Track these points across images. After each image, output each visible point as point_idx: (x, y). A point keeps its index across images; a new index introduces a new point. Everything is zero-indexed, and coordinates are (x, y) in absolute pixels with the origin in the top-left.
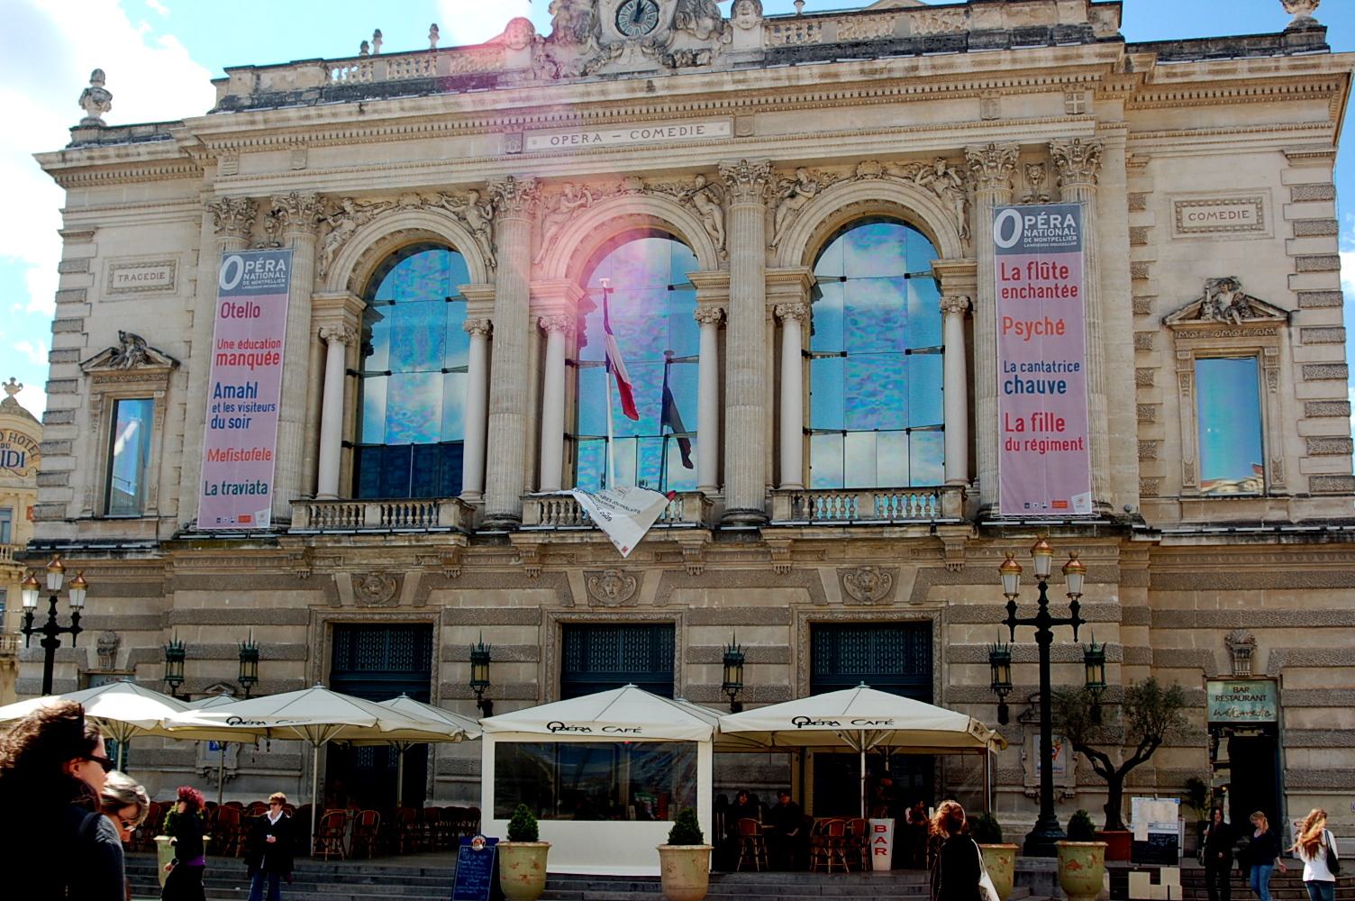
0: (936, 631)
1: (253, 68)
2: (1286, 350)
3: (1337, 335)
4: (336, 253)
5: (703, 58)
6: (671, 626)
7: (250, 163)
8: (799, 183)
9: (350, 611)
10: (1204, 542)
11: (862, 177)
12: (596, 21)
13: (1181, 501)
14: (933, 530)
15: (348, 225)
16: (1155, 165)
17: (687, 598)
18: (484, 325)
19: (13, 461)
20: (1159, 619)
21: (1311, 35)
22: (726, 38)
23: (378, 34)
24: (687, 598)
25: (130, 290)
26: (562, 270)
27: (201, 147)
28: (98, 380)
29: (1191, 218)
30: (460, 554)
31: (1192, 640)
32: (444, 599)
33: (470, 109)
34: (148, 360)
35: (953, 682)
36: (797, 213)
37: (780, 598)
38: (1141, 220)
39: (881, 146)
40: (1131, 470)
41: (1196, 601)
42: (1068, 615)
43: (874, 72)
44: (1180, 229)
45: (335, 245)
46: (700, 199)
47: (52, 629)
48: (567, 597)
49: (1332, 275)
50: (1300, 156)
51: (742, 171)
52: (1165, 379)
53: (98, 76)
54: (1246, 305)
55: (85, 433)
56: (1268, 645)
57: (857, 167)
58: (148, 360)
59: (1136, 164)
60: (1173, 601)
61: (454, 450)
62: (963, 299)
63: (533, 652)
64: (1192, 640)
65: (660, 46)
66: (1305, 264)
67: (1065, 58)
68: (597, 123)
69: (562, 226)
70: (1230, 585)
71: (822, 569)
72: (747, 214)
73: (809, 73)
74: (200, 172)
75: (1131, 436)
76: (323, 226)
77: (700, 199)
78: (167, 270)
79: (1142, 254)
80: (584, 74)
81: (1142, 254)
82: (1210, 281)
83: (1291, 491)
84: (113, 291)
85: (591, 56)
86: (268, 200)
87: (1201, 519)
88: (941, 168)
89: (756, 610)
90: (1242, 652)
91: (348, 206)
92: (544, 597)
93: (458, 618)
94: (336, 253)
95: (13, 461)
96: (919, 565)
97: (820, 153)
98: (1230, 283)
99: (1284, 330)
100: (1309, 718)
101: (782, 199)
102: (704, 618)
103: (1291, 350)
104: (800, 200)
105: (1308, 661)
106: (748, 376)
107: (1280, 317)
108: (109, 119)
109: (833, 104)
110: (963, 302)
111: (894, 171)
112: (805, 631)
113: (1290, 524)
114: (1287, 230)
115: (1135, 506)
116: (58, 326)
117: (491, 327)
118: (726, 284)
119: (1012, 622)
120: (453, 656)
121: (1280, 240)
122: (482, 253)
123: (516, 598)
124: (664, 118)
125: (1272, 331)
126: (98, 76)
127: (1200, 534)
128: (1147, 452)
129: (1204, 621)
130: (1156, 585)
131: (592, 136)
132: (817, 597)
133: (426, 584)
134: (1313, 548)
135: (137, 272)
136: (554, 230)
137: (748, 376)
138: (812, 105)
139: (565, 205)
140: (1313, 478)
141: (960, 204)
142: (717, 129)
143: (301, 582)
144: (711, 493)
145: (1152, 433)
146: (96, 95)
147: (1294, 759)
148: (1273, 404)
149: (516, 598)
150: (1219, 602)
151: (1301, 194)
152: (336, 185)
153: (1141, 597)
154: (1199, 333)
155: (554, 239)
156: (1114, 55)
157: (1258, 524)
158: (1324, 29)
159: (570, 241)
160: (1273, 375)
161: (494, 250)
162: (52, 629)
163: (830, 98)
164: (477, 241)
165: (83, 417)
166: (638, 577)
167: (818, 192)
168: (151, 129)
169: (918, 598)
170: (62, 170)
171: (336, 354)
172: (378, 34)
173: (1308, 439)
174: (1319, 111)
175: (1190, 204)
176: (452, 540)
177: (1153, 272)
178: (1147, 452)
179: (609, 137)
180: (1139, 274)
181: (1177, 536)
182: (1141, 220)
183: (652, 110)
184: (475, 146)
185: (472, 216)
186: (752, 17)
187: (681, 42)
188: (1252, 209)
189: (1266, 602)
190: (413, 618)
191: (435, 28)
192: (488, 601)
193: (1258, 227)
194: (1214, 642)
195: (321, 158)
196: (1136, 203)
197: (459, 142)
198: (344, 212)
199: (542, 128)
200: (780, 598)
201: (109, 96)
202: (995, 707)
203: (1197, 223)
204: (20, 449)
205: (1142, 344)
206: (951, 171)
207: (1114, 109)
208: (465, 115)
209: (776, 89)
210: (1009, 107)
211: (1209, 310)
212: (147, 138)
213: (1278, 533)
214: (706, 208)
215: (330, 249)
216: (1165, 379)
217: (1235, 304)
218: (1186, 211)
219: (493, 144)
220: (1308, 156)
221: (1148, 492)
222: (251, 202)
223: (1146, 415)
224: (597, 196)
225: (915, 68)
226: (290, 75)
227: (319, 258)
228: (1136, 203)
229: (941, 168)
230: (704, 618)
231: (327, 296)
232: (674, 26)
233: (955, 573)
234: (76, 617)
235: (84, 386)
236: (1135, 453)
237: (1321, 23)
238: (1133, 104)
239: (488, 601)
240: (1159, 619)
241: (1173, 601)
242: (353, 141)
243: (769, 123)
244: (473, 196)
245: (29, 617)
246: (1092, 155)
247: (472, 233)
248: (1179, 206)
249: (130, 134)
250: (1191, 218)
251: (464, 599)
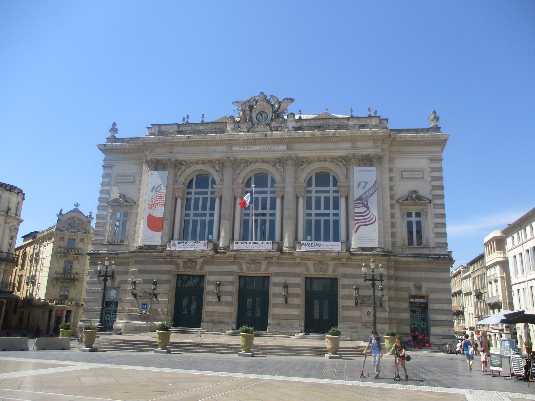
0: (338, 280)
1: (159, 125)
2: (429, 210)
3: (443, 206)
4: (180, 175)
5: (279, 129)
6: (269, 277)
7: (157, 150)
8: (303, 162)
9: (182, 271)
10: (408, 259)
11: (320, 161)
12: (251, 118)
13: (403, 247)
14: (339, 254)
15: (183, 168)
16: (396, 161)
17: (273, 270)
18: (220, 196)
19: (76, 225)
20: (397, 278)
21: (437, 129)
22: (286, 124)
23: (188, 116)
24: (273, 270)
25: (122, 182)
26: (241, 182)
27: (145, 145)
28: (112, 206)
29: (405, 175)
30: (213, 257)
31: (405, 284)
32: (208, 268)
33: (218, 139)
34: (127, 201)
35: (343, 294)
36: (303, 170)
37: (298, 270)
38: (392, 175)
39: (326, 154)
40: (389, 239)
41: (406, 274)
42: (380, 278)
43: (324, 134)
44: (402, 178)
45: (180, 173)
46: (277, 165)
47: (106, 276)
48: (241, 269)
49: (441, 191)
50: (434, 160)
51: (289, 158)
52: (398, 216)
53: (115, 124)
54: (419, 198)
55: (109, 220)
56: (425, 286)
58: (127, 201)
59: (391, 160)
60: (400, 274)
62: (346, 194)
63: (232, 283)
64: (405, 284)
65: (269, 125)
66: (434, 188)
67: (374, 133)
68: (251, 144)
69: (241, 170)
70: (415, 270)
71: (309, 262)
72: (290, 169)
73: (308, 133)
74: (143, 152)
75: (389, 231)
76: (177, 168)
77: (277, 165)
78: (132, 178)
79: (393, 184)
80: (248, 131)
81: (393, 184)
82: (410, 191)
83: (431, 246)
84: (117, 183)
85: (250, 126)
86: (162, 160)
87: (407, 253)
88: (340, 160)
89: (291, 273)
90: (419, 288)
91: (184, 163)
92: (235, 268)
93: (211, 273)
94: (180, 175)
95: (76, 225)
96: (334, 262)
97: (310, 155)
98: (415, 192)
99: (429, 205)
100: (436, 306)
101: (299, 166)
102: (277, 275)
103: (431, 210)
104: (304, 166)
105: (435, 290)
106: (289, 212)
107: (428, 201)
108: (117, 136)
109: (313, 142)
110: (346, 194)
111: (328, 160)
112: (304, 279)
113: (430, 255)
114: (429, 179)
115: (390, 249)
116: (101, 192)
117: (222, 196)
118: (284, 187)
119: (365, 280)
120: (211, 283)
121: (428, 181)
122: (220, 176)
123: (228, 268)
124: (269, 144)
125: (426, 205)
126: (115, 124)
127: (407, 257)
128: (393, 234)
129: (408, 279)
130: (396, 269)
131: (250, 147)
132: (308, 270)
133: (203, 264)
134: (436, 261)
135: (124, 178)
136: (239, 171)
137: (289, 212)
138: (308, 142)
139: (242, 165)
140: (437, 243)
141: (345, 169)
142: (283, 147)
143: (171, 263)
144: (280, 242)
145: (395, 230)
146: (114, 129)
147: (432, 316)
148: (426, 224)
149: (228, 268)
150: (412, 274)
151: (434, 170)
152: (181, 157)
153: (392, 272)
154: (407, 205)
155: (239, 174)
156: (387, 133)
157: (422, 254)
158: (440, 128)
159: (243, 175)
160: (426, 216)
161: (223, 176)
162: (106, 276)
163: (313, 140)
164: (218, 174)
166: (260, 263)
167: (308, 164)
168: (129, 139)
169: (334, 271)
170: (104, 149)
171: (179, 202)
172: (188, 116)
173: (436, 233)
174: (439, 149)
175: (404, 171)
176: (211, 252)
177: (395, 188)
178: (393, 234)
179: (254, 148)
180: (391, 188)
181: (401, 257)
182: (392, 175)
183: (266, 141)
184: (219, 148)
185: (217, 167)
186: (293, 119)
188: (421, 173)
189: (424, 275)
190: (199, 274)
191: (203, 115)
192: (219, 269)
193: (422, 178)
194: (411, 285)
195: (177, 149)
196: (391, 170)
197: (214, 148)
198: (182, 164)
199: (237, 145)
200: (298, 270)
201: (117, 130)
202: (354, 301)
203: (406, 176)
204: (78, 222)
205: (392, 206)
206: (343, 161)
207: (386, 146)
208: (216, 141)
209: (299, 138)
210: (359, 144)
211: (409, 199)
212: (128, 141)
213: (428, 257)
214: (279, 167)
215: (179, 174)
216: (398, 216)
217: (416, 197)
218: (404, 173)
219: (224, 148)
220: (435, 160)
221: (394, 245)
222: (158, 161)
223: (393, 225)
224: (250, 163)
225: (335, 134)
226: (169, 127)
227: (175, 176)
228: (391, 170)
229: (340, 160)
230: (277, 275)
231: (178, 186)
232: (272, 120)
233: (344, 265)
234: (113, 273)
236: (390, 234)
237: (439, 126)
238: (391, 145)
239: (219, 269)
240: (397, 278)
241: (400, 274)
242: (186, 146)
243: (296, 146)
244: (217, 162)
245: (100, 273)
246: (380, 158)
247: (217, 171)
248: (402, 172)
249: (122, 140)
250: (405, 175)
251: (213, 268)
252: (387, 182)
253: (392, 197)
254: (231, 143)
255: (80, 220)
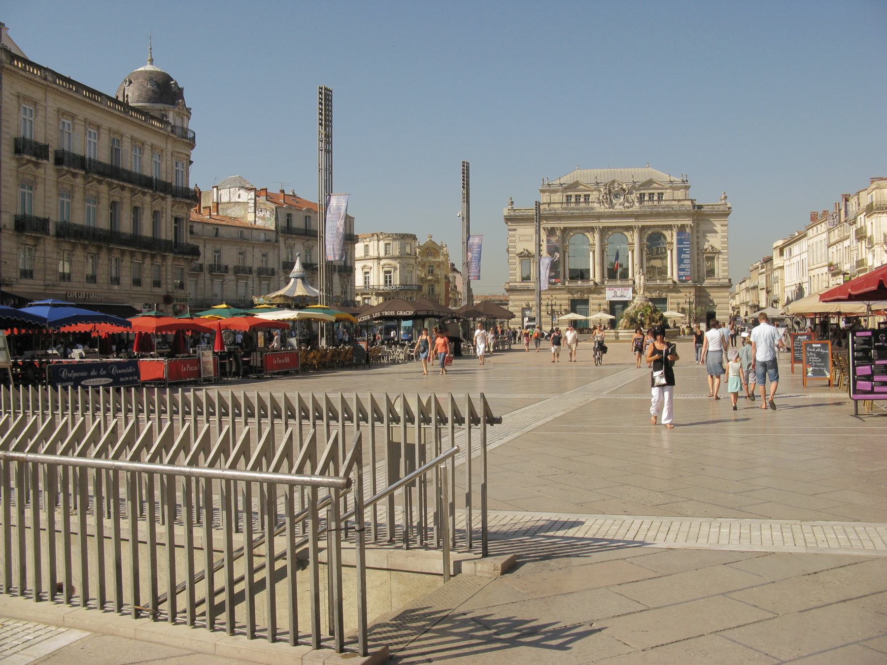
57: (654, 226)
59: (698, 225)
61: (589, 270)
108: (515, 207)
165: (517, 263)
180: (698, 243)
187: (626, 204)
189: (715, 294)
196: (698, 232)
205: (698, 254)
228: (698, 232)
235: (517, 258)
252: (695, 240)
253: (698, 249)
254: (599, 216)
255: (434, 249)
